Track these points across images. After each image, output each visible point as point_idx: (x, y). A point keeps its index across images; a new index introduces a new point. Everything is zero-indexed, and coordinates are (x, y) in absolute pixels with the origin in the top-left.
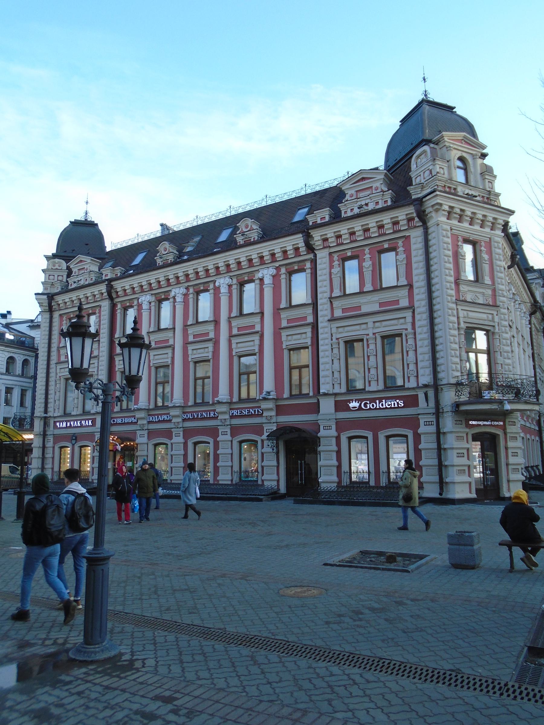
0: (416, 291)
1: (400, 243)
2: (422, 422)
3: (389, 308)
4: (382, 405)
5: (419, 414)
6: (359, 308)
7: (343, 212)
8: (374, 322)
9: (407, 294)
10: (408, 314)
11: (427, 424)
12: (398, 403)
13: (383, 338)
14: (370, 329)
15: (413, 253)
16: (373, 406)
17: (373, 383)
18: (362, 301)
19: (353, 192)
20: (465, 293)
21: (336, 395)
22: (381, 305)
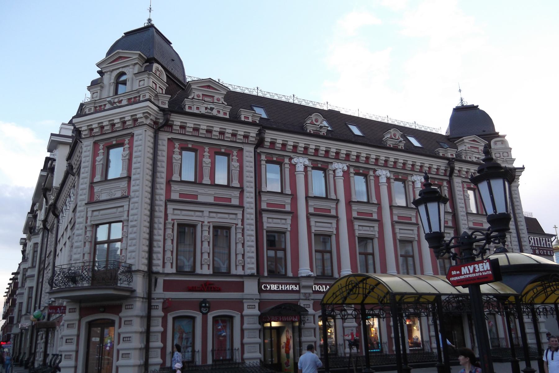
0: (246, 194)
1: (235, 153)
2: (245, 306)
3: (221, 203)
5: (243, 299)
6: (196, 196)
7: (187, 107)
8: (210, 212)
9: (238, 195)
10: (239, 212)
11: (250, 307)
13: (214, 227)
14: (206, 218)
15: (245, 164)
17: (205, 267)
18: (200, 191)
22: (216, 198)
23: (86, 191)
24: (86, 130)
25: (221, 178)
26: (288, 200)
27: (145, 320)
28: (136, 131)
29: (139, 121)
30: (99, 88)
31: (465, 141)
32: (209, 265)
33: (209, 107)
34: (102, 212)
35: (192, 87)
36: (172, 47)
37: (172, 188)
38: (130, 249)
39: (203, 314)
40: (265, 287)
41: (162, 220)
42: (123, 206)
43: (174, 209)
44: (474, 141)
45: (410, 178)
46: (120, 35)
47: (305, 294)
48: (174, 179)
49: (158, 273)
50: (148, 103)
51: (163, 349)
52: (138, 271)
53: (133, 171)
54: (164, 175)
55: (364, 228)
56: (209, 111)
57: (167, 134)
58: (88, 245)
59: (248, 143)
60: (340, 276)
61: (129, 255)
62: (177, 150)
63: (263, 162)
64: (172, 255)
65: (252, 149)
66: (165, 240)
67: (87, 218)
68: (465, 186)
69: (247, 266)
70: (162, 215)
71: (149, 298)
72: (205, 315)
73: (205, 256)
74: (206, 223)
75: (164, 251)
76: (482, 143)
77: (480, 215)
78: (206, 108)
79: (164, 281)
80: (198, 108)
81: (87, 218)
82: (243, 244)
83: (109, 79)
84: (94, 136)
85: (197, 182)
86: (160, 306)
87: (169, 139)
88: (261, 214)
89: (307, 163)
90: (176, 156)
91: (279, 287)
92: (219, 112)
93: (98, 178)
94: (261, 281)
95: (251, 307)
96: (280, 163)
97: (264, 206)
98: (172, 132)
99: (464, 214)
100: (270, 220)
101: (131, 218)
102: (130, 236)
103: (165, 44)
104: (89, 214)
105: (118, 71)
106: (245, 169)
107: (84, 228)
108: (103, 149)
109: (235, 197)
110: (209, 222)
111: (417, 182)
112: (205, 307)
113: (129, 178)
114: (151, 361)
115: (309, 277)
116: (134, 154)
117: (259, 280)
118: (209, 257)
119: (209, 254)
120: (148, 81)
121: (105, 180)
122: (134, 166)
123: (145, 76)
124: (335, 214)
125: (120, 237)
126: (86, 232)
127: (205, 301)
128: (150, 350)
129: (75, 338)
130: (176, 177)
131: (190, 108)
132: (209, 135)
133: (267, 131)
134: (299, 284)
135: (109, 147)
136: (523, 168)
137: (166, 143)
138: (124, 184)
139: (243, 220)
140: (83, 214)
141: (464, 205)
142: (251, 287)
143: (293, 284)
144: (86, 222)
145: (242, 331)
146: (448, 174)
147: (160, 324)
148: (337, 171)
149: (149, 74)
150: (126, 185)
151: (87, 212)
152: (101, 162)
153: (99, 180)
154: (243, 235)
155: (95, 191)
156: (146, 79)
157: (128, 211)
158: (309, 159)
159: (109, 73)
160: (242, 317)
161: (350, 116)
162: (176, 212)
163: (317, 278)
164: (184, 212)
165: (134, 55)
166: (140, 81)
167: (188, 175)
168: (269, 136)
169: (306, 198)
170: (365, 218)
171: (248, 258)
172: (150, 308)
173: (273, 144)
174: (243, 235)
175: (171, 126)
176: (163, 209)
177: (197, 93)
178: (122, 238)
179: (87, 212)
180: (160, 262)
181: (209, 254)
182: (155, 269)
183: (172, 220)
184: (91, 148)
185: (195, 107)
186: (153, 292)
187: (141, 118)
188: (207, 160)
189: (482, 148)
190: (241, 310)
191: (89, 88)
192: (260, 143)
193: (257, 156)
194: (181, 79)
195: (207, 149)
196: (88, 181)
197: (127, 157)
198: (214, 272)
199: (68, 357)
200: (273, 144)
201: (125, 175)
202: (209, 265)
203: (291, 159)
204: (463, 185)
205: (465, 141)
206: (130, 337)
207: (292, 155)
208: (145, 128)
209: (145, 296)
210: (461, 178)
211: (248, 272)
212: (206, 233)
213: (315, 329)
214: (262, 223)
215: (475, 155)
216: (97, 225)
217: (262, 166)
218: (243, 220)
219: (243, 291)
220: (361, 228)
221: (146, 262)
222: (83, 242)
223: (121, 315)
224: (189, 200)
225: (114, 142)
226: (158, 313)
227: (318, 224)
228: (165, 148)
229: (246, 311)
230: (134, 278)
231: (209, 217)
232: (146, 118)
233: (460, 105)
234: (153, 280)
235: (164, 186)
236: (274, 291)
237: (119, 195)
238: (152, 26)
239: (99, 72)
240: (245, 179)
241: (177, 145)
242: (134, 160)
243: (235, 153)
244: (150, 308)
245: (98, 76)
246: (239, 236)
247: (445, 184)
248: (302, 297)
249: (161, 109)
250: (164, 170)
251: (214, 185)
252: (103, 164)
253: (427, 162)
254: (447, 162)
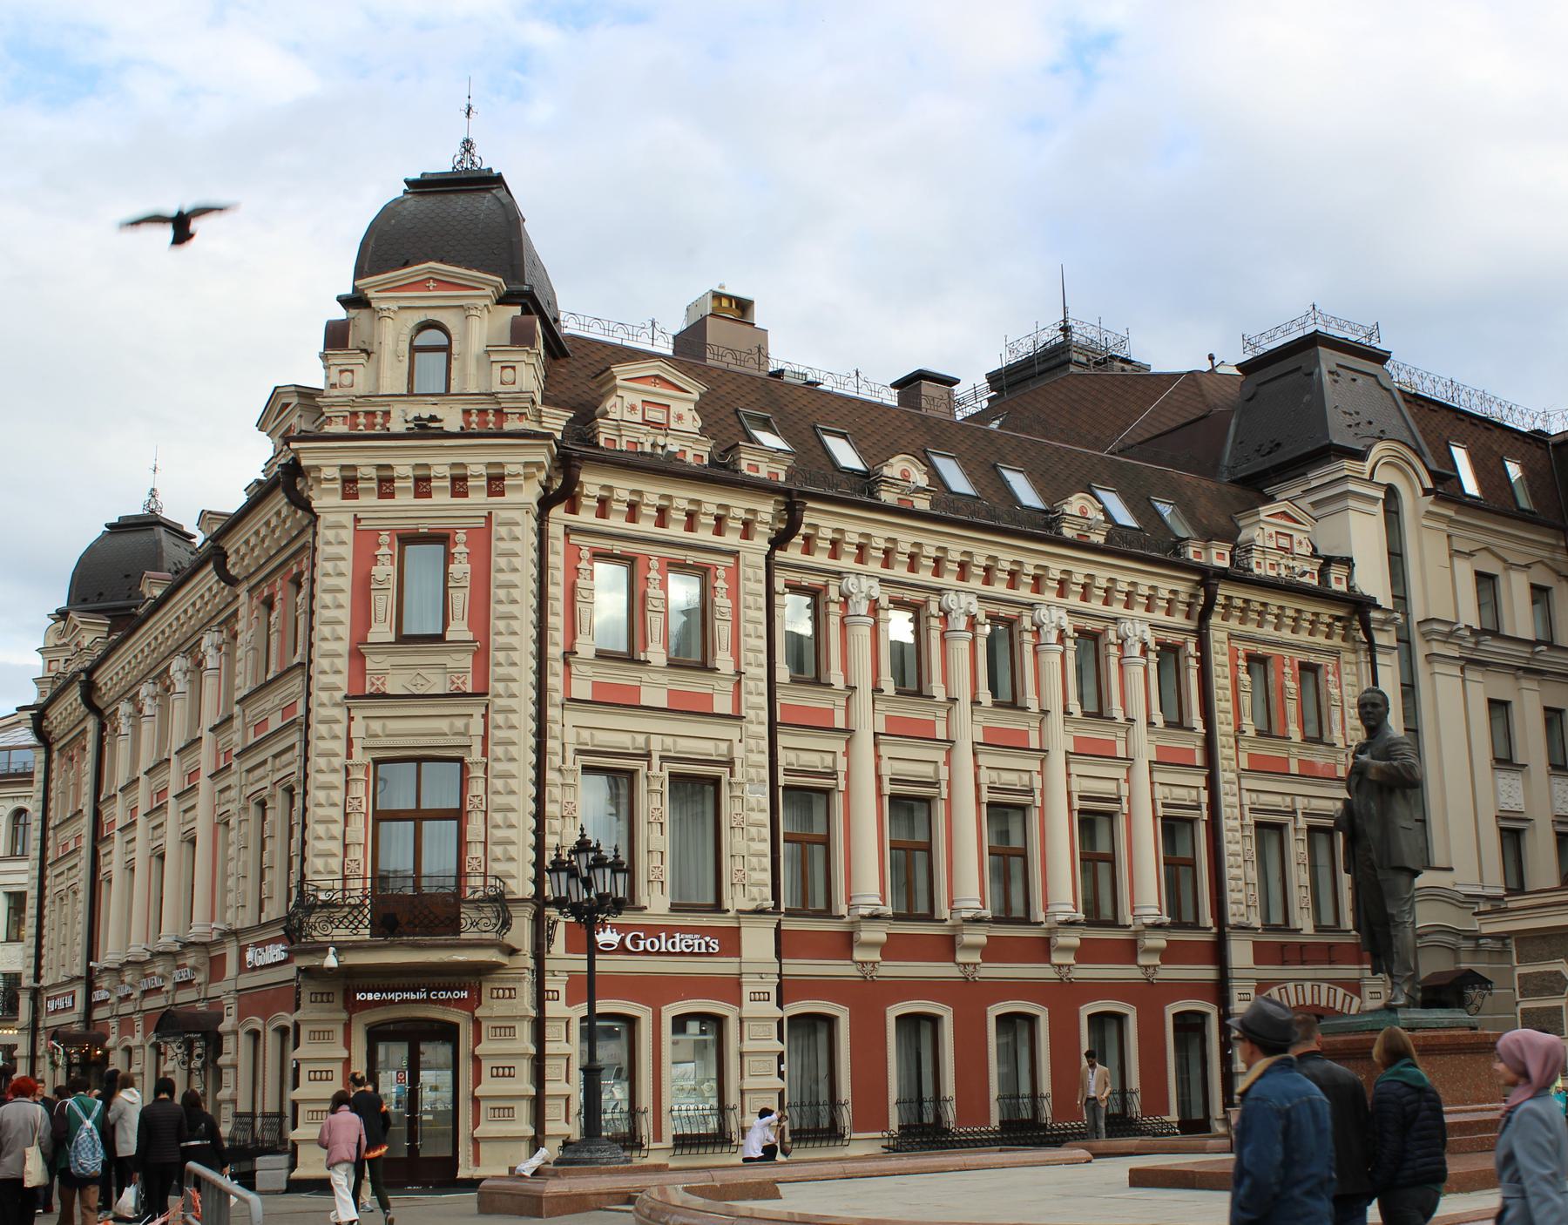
4: (673, 944)
12: (707, 945)
16: (652, 944)
20: (383, 673)
108: (390, 546)
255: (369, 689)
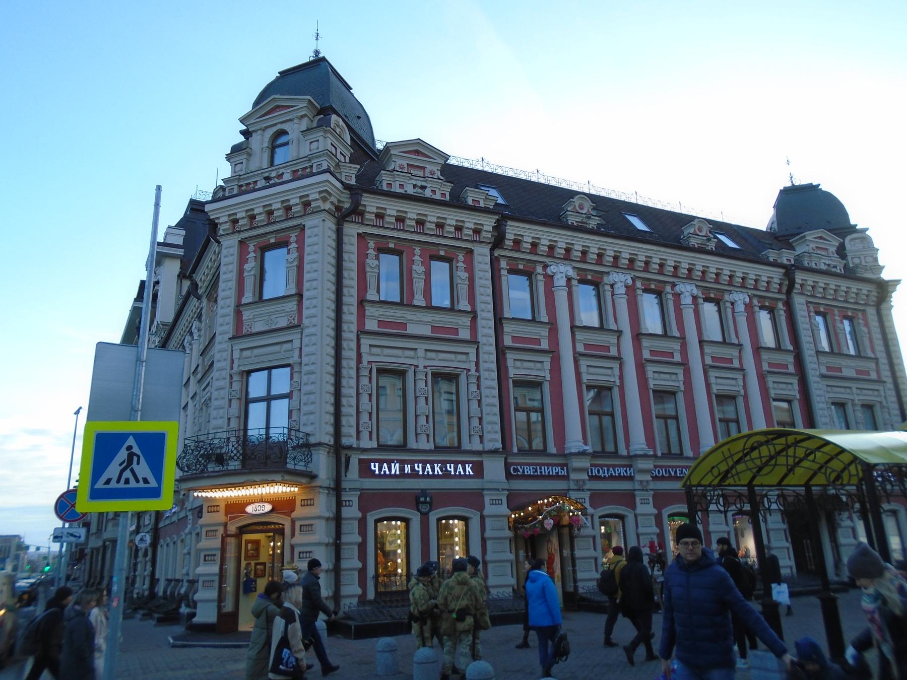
2: (487, 500)
3: (443, 336)
5: (483, 489)
10: (472, 350)
11: (494, 502)
13: (433, 374)
14: (422, 359)
15: (478, 274)
17: (423, 438)
18: (409, 317)
19: (405, 163)
21: (365, 450)
22: (434, 329)
23: (231, 319)
24: (226, 222)
25: (441, 298)
26: (544, 332)
27: (333, 524)
28: (309, 222)
29: (313, 205)
30: (245, 156)
31: (807, 238)
32: (428, 436)
33: (419, 184)
34: (256, 351)
35: (392, 152)
36: (352, 95)
37: (367, 313)
38: (304, 409)
39: (422, 514)
40: (516, 470)
41: (354, 364)
42: (291, 341)
43: (371, 346)
44: (821, 238)
45: (727, 297)
46: (273, 76)
47: (577, 481)
48: (369, 297)
49: (350, 448)
50: (327, 176)
51: (362, 572)
52: (319, 444)
53: (306, 285)
54: (354, 292)
55: (662, 376)
56: (420, 190)
57: (356, 226)
58: (235, 403)
59: (480, 242)
60: (628, 452)
61: (304, 419)
62: (371, 252)
63: (504, 272)
64: (370, 419)
65: (487, 251)
66: (358, 394)
67: (232, 361)
68: (812, 309)
69: (487, 437)
70: (354, 355)
71: (337, 489)
72: (425, 516)
73: (422, 421)
74: (421, 368)
75: (358, 412)
76: (835, 242)
77: (836, 354)
78: (415, 186)
79: (360, 460)
80: (401, 186)
81: (232, 361)
82: (479, 401)
83: (260, 142)
84: (239, 232)
85: (405, 303)
86: (355, 501)
87: (359, 234)
88: (504, 354)
89: (571, 273)
90: (371, 262)
91: (536, 470)
92: (434, 192)
93: (248, 298)
94: (509, 461)
95: (496, 502)
96: (529, 274)
97: (508, 341)
98: (363, 224)
99: (813, 352)
100: (518, 364)
101: (305, 360)
102: (305, 389)
103: (343, 88)
104: (236, 354)
105: (274, 129)
106: (478, 282)
107: (228, 377)
108: (254, 252)
109: (464, 326)
110: (425, 367)
111: (739, 302)
112: (425, 502)
113: (300, 295)
114: (345, 590)
115: (583, 454)
116: (307, 259)
117: (506, 459)
118: (427, 422)
119: (427, 417)
120: (324, 142)
121: (260, 300)
122: (307, 276)
123: (319, 135)
124: (616, 354)
125: (286, 390)
126: (231, 383)
127: (424, 492)
128: (342, 573)
129: (219, 553)
130: (371, 295)
131: (389, 185)
132: (419, 229)
133: (509, 223)
134: (566, 465)
135: (265, 249)
136: (897, 282)
137: (354, 240)
138: (292, 305)
139: (477, 364)
140: (227, 355)
141: (811, 339)
142: (494, 469)
143: (557, 465)
144: (232, 368)
145: (484, 541)
146: (784, 289)
147: (356, 531)
148: (616, 287)
149: (325, 132)
150: (295, 308)
151: (232, 351)
152: (253, 272)
153: (250, 300)
154: (478, 387)
155: (244, 318)
156: (321, 139)
157: (301, 349)
158: (574, 268)
159: (259, 132)
160: (483, 518)
161: (624, 202)
162: (374, 350)
163: (595, 455)
164: (386, 351)
165: (301, 103)
166: (311, 143)
167: (390, 290)
168: (513, 230)
169: (572, 328)
170: (662, 358)
171: (488, 423)
172: (339, 504)
173: (517, 243)
174: (478, 387)
175: (362, 214)
176: (354, 345)
177: (399, 162)
178: (292, 392)
179: (232, 351)
180: (353, 431)
181: (427, 417)
182: (345, 441)
183: (369, 362)
184: (235, 250)
185: (398, 183)
186: (343, 478)
187: (317, 200)
188: (418, 268)
189: (834, 249)
190: (481, 507)
191: (229, 158)
192: (498, 242)
193: (494, 262)
194: (369, 142)
195: (417, 251)
196: (232, 302)
197: (295, 263)
198: (436, 447)
199: (208, 584)
200: (517, 243)
201: (293, 292)
202: (428, 436)
203: (546, 266)
204: (808, 307)
205: (807, 238)
206: (310, 552)
207: (547, 260)
208: (324, 215)
209: (332, 486)
210: (804, 297)
211: (489, 446)
212: (421, 384)
213: (594, 538)
214: (507, 368)
215: (823, 261)
216: (249, 373)
217: (503, 278)
218: (477, 364)
219: (482, 477)
220: (656, 375)
221: (331, 429)
222: (227, 400)
223: (294, 515)
224: (394, 331)
225: (273, 241)
226: (352, 512)
227: (591, 370)
228: (354, 249)
229: (489, 510)
230: (315, 457)
231: (425, 358)
232: (324, 199)
233: (789, 184)
234: (343, 460)
235: (354, 309)
236: (530, 477)
237: (283, 323)
238: (324, 59)
239: (242, 132)
240: (479, 298)
241: (371, 244)
242: (307, 267)
243: (461, 257)
244: (339, 504)
245: (242, 139)
246: (473, 388)
247: (780, 305)
248: (573, 486)
249: (346, 187)
250: (354, 283)
251: (430, 308)
252: (255, 275)
253: (753, 271)
254: (783, 271)
255: (245, 331)
